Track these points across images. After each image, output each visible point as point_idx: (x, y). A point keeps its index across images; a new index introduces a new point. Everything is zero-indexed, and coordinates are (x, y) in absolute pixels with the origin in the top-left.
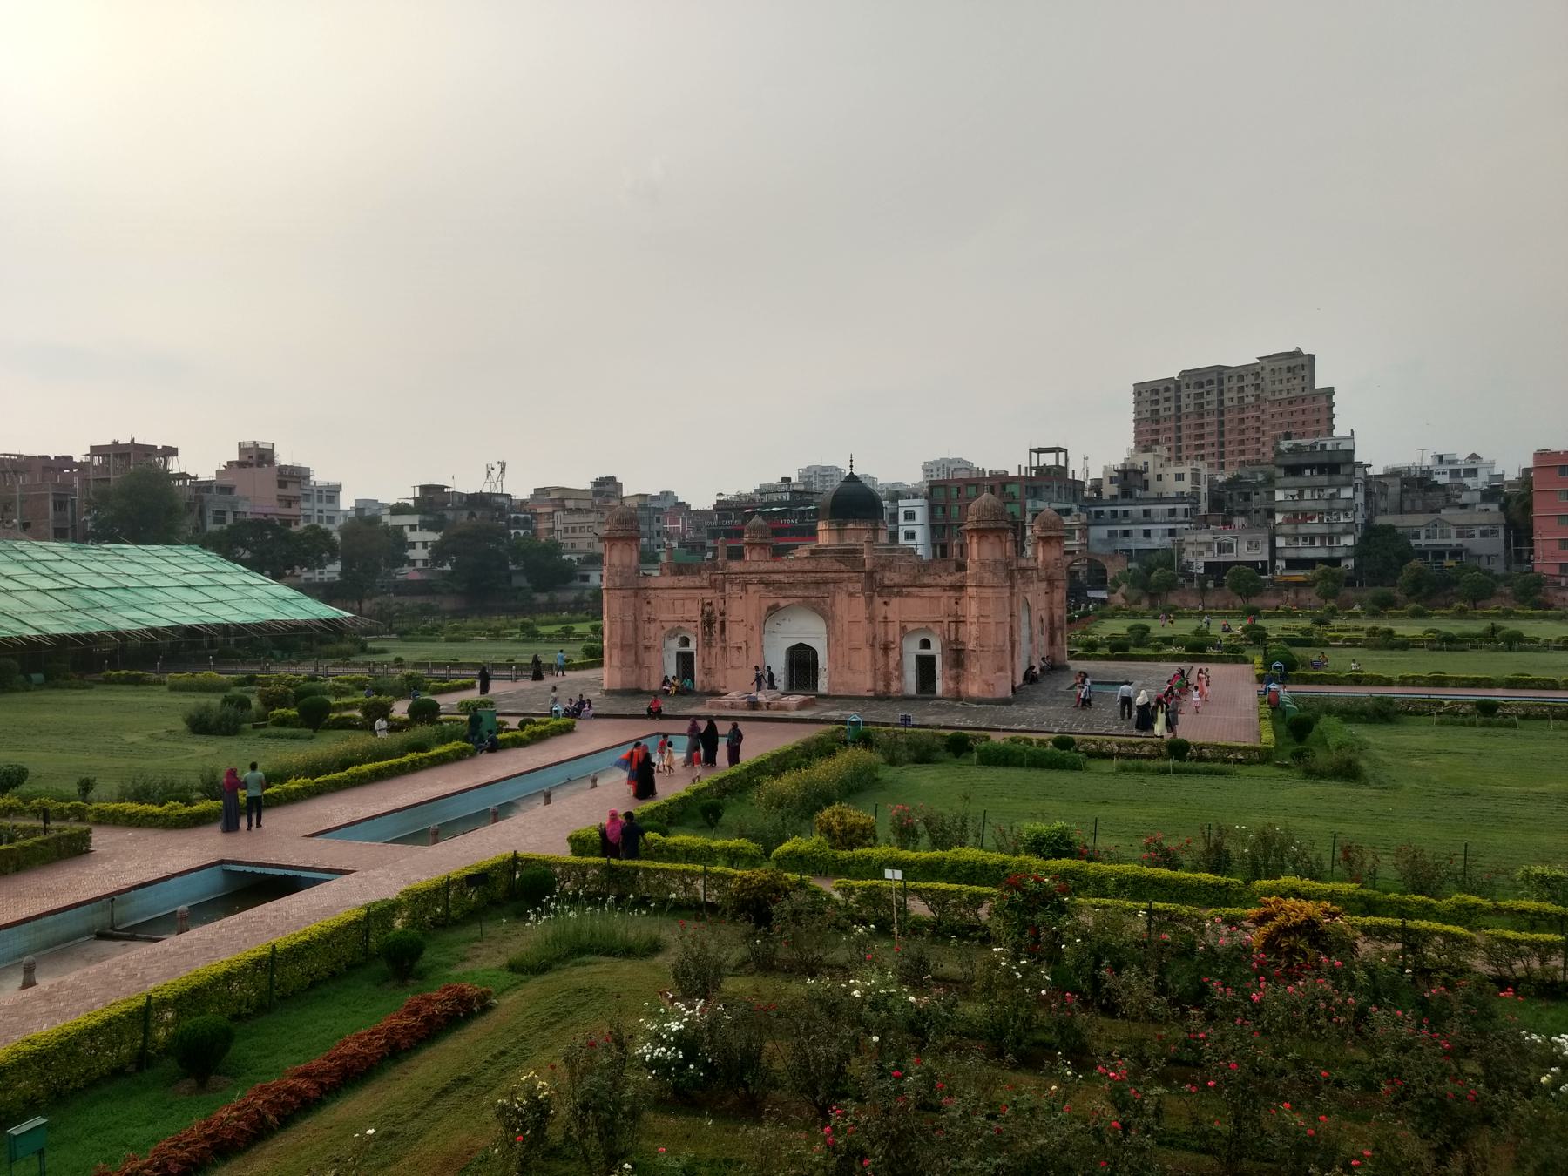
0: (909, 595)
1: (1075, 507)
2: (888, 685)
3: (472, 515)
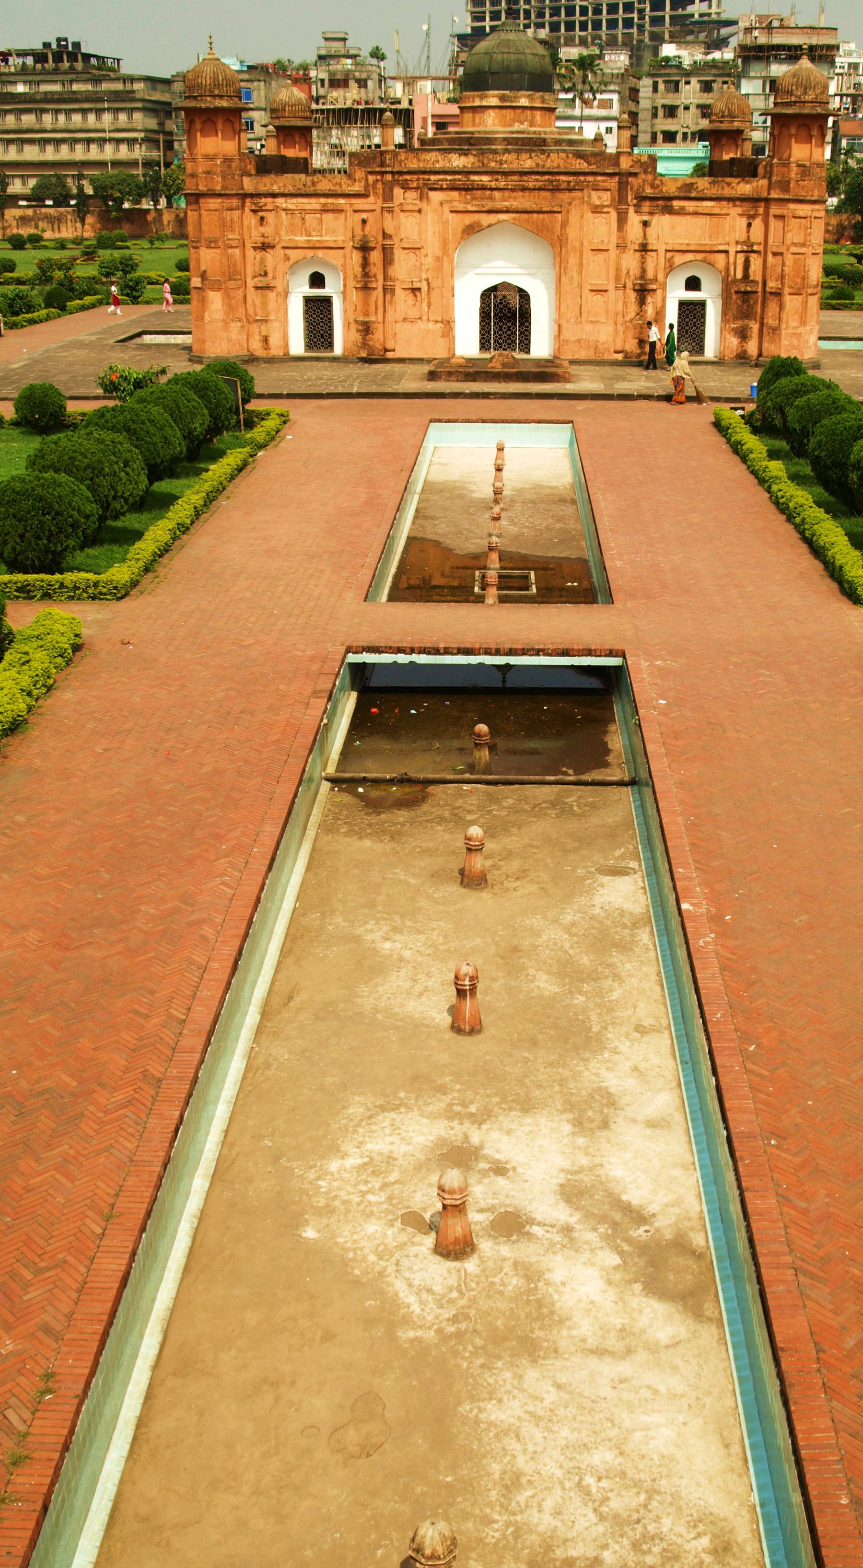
0: (681, 212)
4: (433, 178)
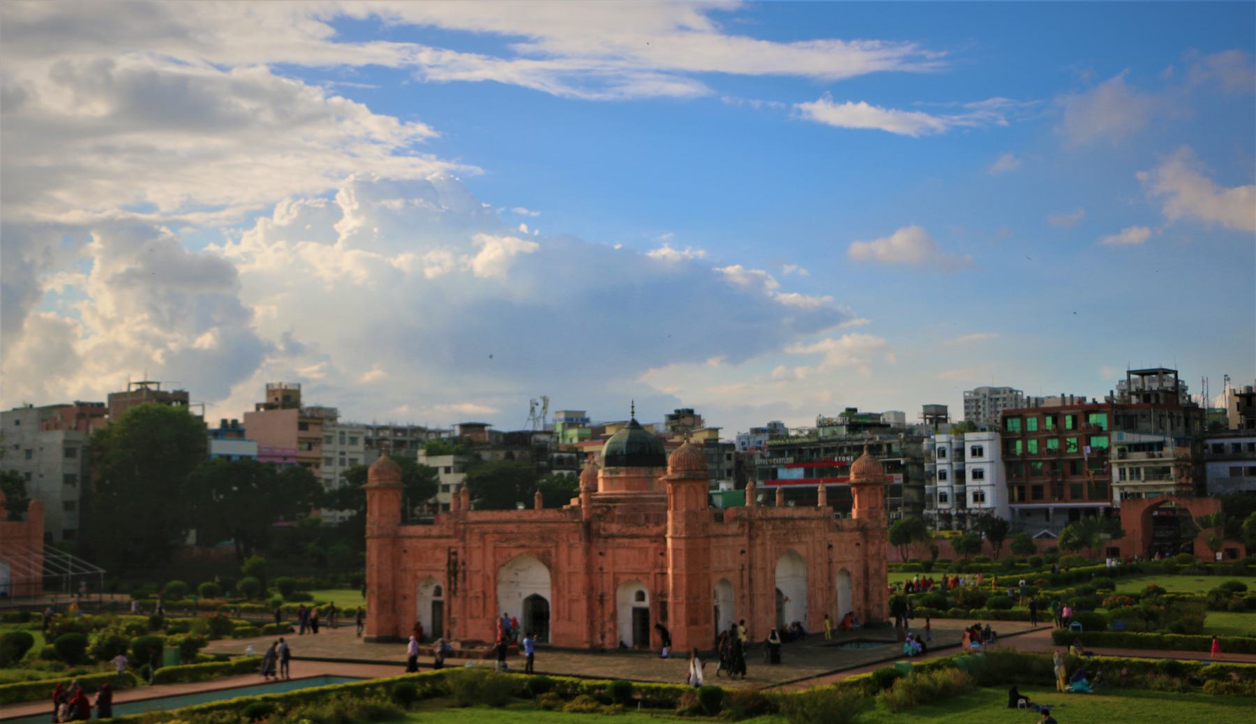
1: (1169, 440)
2: (603, 637)
3: (510, 456)
4: (486, 526)
